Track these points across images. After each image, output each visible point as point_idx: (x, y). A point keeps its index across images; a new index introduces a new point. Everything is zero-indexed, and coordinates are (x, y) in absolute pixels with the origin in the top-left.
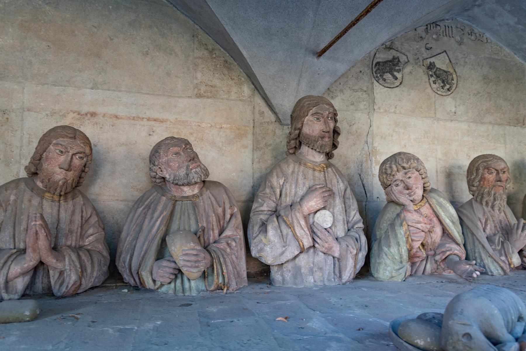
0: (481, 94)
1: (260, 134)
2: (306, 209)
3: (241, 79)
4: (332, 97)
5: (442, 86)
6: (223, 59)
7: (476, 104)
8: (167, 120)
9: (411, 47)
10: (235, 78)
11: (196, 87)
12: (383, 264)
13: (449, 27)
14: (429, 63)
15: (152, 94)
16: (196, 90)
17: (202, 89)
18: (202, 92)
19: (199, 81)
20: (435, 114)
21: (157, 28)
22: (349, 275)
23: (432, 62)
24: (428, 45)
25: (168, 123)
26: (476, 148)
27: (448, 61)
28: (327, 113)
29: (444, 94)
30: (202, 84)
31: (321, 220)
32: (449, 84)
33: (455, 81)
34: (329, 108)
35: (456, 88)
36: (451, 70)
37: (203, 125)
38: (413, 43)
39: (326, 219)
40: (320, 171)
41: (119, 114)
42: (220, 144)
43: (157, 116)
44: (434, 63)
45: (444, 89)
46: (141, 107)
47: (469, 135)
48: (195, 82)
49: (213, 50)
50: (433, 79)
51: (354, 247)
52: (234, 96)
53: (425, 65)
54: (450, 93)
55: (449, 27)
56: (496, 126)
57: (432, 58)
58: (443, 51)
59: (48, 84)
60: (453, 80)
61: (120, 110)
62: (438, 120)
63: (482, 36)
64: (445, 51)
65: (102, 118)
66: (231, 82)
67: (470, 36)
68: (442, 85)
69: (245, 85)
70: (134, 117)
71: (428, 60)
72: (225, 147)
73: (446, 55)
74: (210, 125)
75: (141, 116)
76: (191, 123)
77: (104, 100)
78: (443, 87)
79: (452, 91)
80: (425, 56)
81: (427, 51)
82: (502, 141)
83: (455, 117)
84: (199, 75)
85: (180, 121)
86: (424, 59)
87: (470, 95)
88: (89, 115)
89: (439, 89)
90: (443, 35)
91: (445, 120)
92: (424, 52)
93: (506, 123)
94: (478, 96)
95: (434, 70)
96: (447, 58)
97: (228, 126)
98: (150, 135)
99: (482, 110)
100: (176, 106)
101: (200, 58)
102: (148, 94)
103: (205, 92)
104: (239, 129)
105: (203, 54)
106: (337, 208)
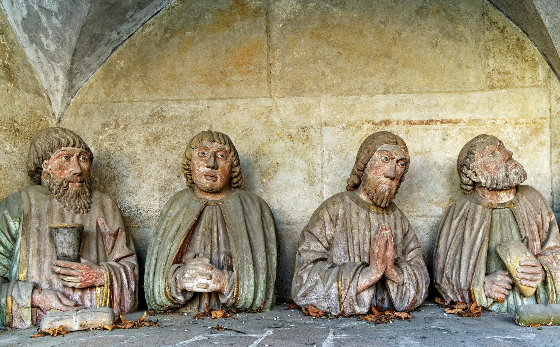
1: (557, 126)
3: (535, 60)
6: (516, 37)
8: (461, 120)
11: (489, 76)
15: (444, 92)
16: (489, 80)
17: (495, 79)
18: (495, 82)
19: (491, 69)
25: (462, 123)
41: (412, 119)
42: (516, 143)
43: (450, 116)
46: (434, 108)
48: (488, 70)
52: (528, 82)
59: (342, 94)
61: (413, 115)
65: (396, 126)
66: (525, 65)
70: (427, 121)
72: (521, 146)
75: (434, 119)
77: (396, 105)
84: (491, 61)
85: (474, 120)
88: (383, 124)
98: (444, 140)
100: (468, 103)
101: (491, 40)
102: (440, 92)
103: (498, 82)
104: (535, 123)
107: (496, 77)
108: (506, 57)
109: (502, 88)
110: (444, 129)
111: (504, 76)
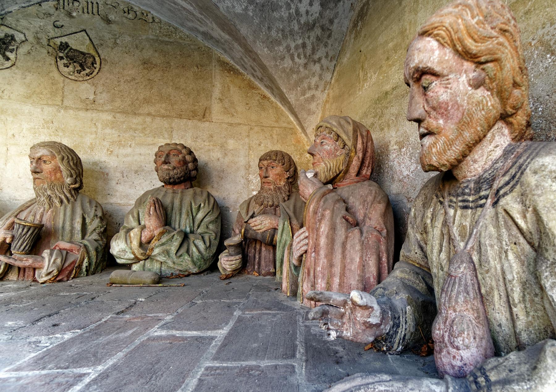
0: (137, 81)
5: (77, 71)
7: (130, 92)
9: (31, 24)
13: (93, 3)
14: (59, 44)
20: (62, 101)
23: (64, 42)
24: (58, 23)
26: (123, 142)
27: (88, 42)
29: (81, 79)
32: (88, 68)
33: (97, 66)
35: (97, 73)
36: (92, 52)
38: (35, 19)
44: (66, 43)
45: (80, 73)
47: (113, 128)
50: (65, 61)
53: (51, 44)
54: (88, 78)
55: (93, 3)
56: (159, 118)
57: (64, 38)
58: (80, 30)
60: (96, 64)
62: (66, 108)
63: (145, 14)
64: (85, 31)
67: (126, 15)
68: (79, 68)
71: (56, 39)
73: (86, 35)
78: (79, 72)
79: (93, 75)
80: (52, 34)
81: (56, 29)
82: (166, 136)
83: (93, 105)
86: (52, 38)
87: (119, 82)
89: (71, 73)
90: (83, 12)
91: (77, 108)
92: (51, 30)
93: (175, 115)
94: (132, 83)
95: (66, 51)
96: (88, 38)
99: (137, 99)
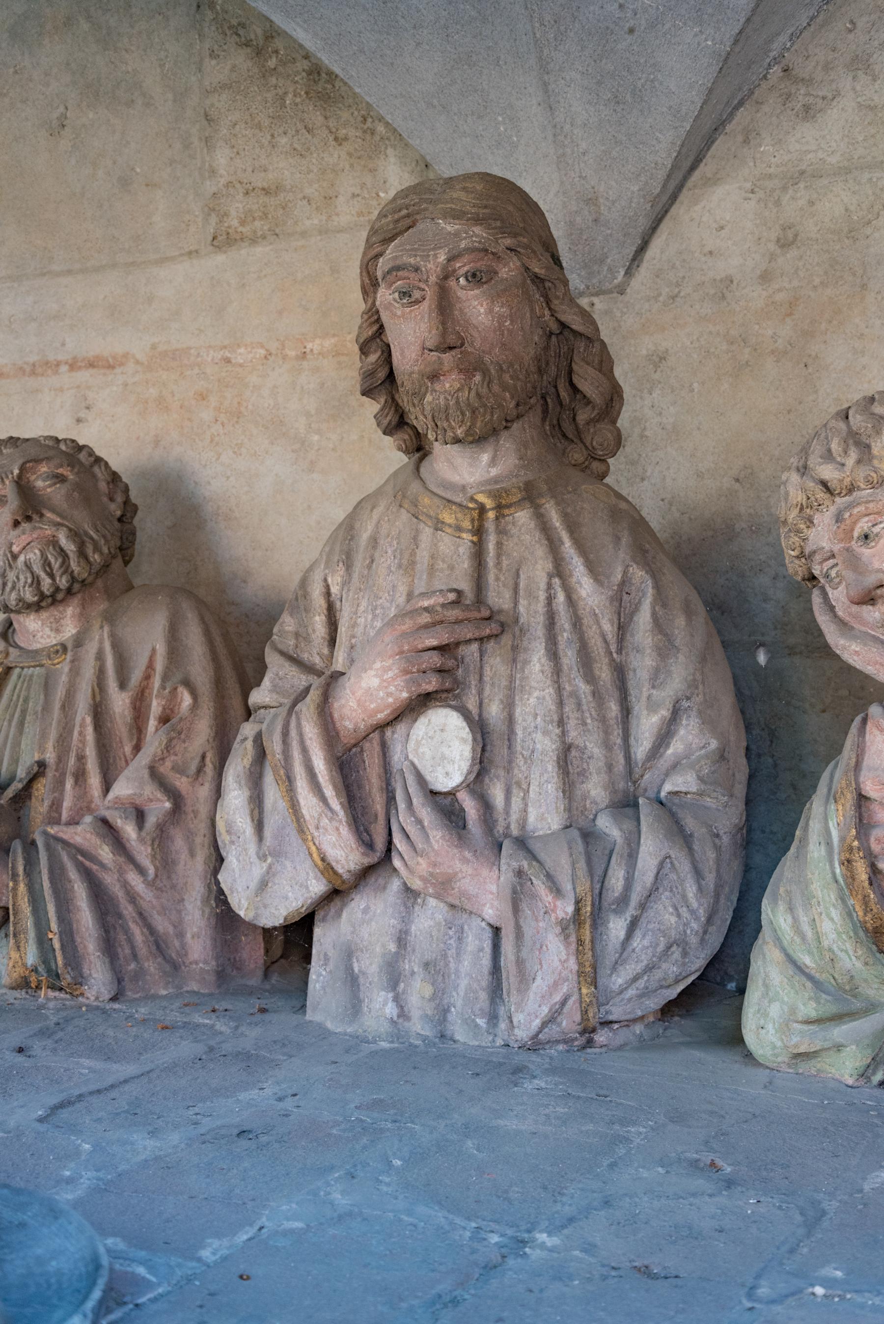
2: (353, 704)
4: (807, 108)
8: (126, 355)
10: (352, 132)
12: (760, 982)
16: (213, 220)
17: (233, 213)
19: (223, 181)
21: (89, 17)
22: (545, 1010)
25: (131, 367)
28: (442, 258)
30: (231, 191)
31: (428, 754)
34: (457, 234)
37: (241, 355)
39: (445, 750)
40: (459, 529)
48: (210, 187)
49: (267, 38)
51: (568, 887)
66: (336, 156)
69: (390, 151)
70: (34, 365)
74: (263, 352)
75: (51, 357)
76: (198, 355)
84: (222, 157)
97: (328, 343)
98: (79, 421)
100: (150, 300)
102: (69, 272)
103: (243, 223)
105: (233, 68)
106: (532, 701)
107: (236, 207)
108: (273, 136)
109: (254, 241)
110: (78, 387)
111: (263, 199)
